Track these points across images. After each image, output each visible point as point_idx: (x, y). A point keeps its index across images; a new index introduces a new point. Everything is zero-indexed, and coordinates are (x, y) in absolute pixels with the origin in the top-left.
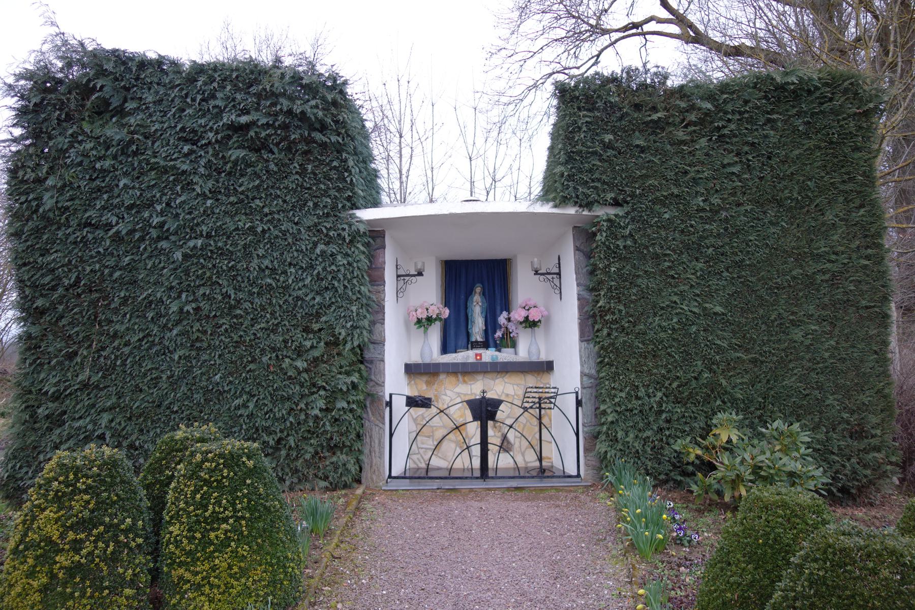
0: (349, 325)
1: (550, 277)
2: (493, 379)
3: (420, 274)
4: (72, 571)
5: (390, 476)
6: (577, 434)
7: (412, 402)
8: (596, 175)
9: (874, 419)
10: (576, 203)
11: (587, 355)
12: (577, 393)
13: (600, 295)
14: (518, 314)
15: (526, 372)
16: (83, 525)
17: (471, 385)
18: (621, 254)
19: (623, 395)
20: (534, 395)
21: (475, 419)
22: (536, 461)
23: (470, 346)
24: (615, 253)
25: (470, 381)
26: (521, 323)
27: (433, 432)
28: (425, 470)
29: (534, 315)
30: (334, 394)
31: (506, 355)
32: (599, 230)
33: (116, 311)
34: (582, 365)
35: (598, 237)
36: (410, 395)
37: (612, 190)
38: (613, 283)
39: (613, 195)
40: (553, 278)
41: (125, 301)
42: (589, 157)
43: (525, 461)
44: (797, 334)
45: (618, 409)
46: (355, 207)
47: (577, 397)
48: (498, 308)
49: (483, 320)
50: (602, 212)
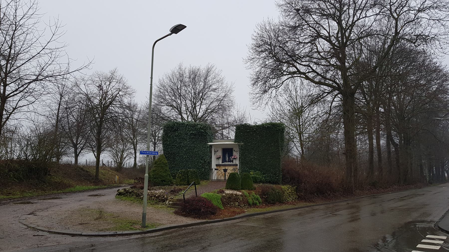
3: (218, 151)
4: (182, 179)
7: (215, 169)
9: (277, 173)
16: (183, 175)
29: (235, 157)
30: (205, 169)
31: (232, 163)
33: (177, 157)
41: (178, 156)
44: (267, 161)
46: (208, 143)
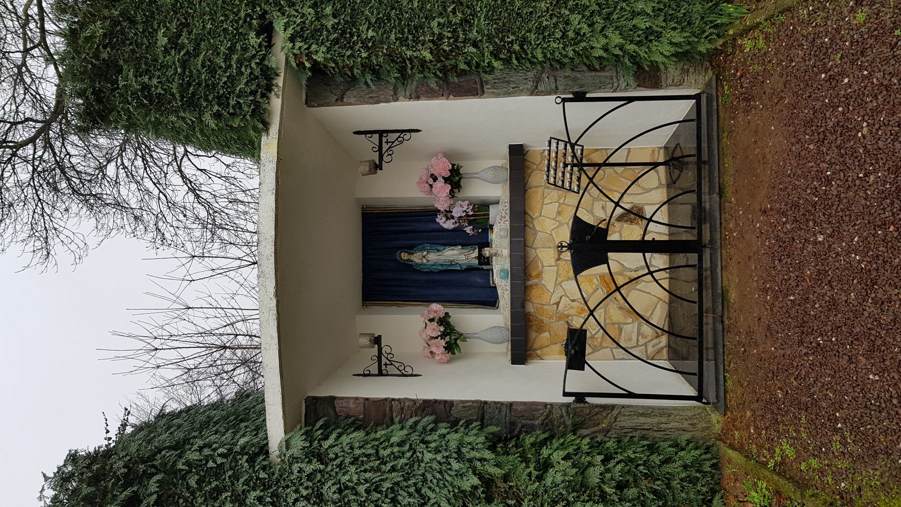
0: (456, 465)
1: (385, 147)
2: (535, 234)
3: (377, 340)
5: (698, 399)
6: (630, 100)
8: (220, 61)
10: (263, 95)
11: (505, 85)
12: (564, 100)
13: (410, 59)
14: (440, 196)
15: (525, 185)
17: (543, 266)
18: (346, 22)
19: (575, 18)
20: (560, 174)
21: (605, 261)
22: (657, 172)
23: (485, 267)
24: (344, 32)
25: (538, 267)
26: (452, 193)
27: (613, 324)
28: (673, 338)
32: (309, 58)
34: (520, 92)
35: (319, 58)
36: (563, 362)
37: (244, 36)
38: (393, 37)
39: (252, 34)
40: (387, 142)
42: (191, 72)
43: (657, 188)
45: (598, 27)
46: (264, 450)
47: (570, 100)
48: (432, 226)
49: (447, 248)
50: (279, 58)
